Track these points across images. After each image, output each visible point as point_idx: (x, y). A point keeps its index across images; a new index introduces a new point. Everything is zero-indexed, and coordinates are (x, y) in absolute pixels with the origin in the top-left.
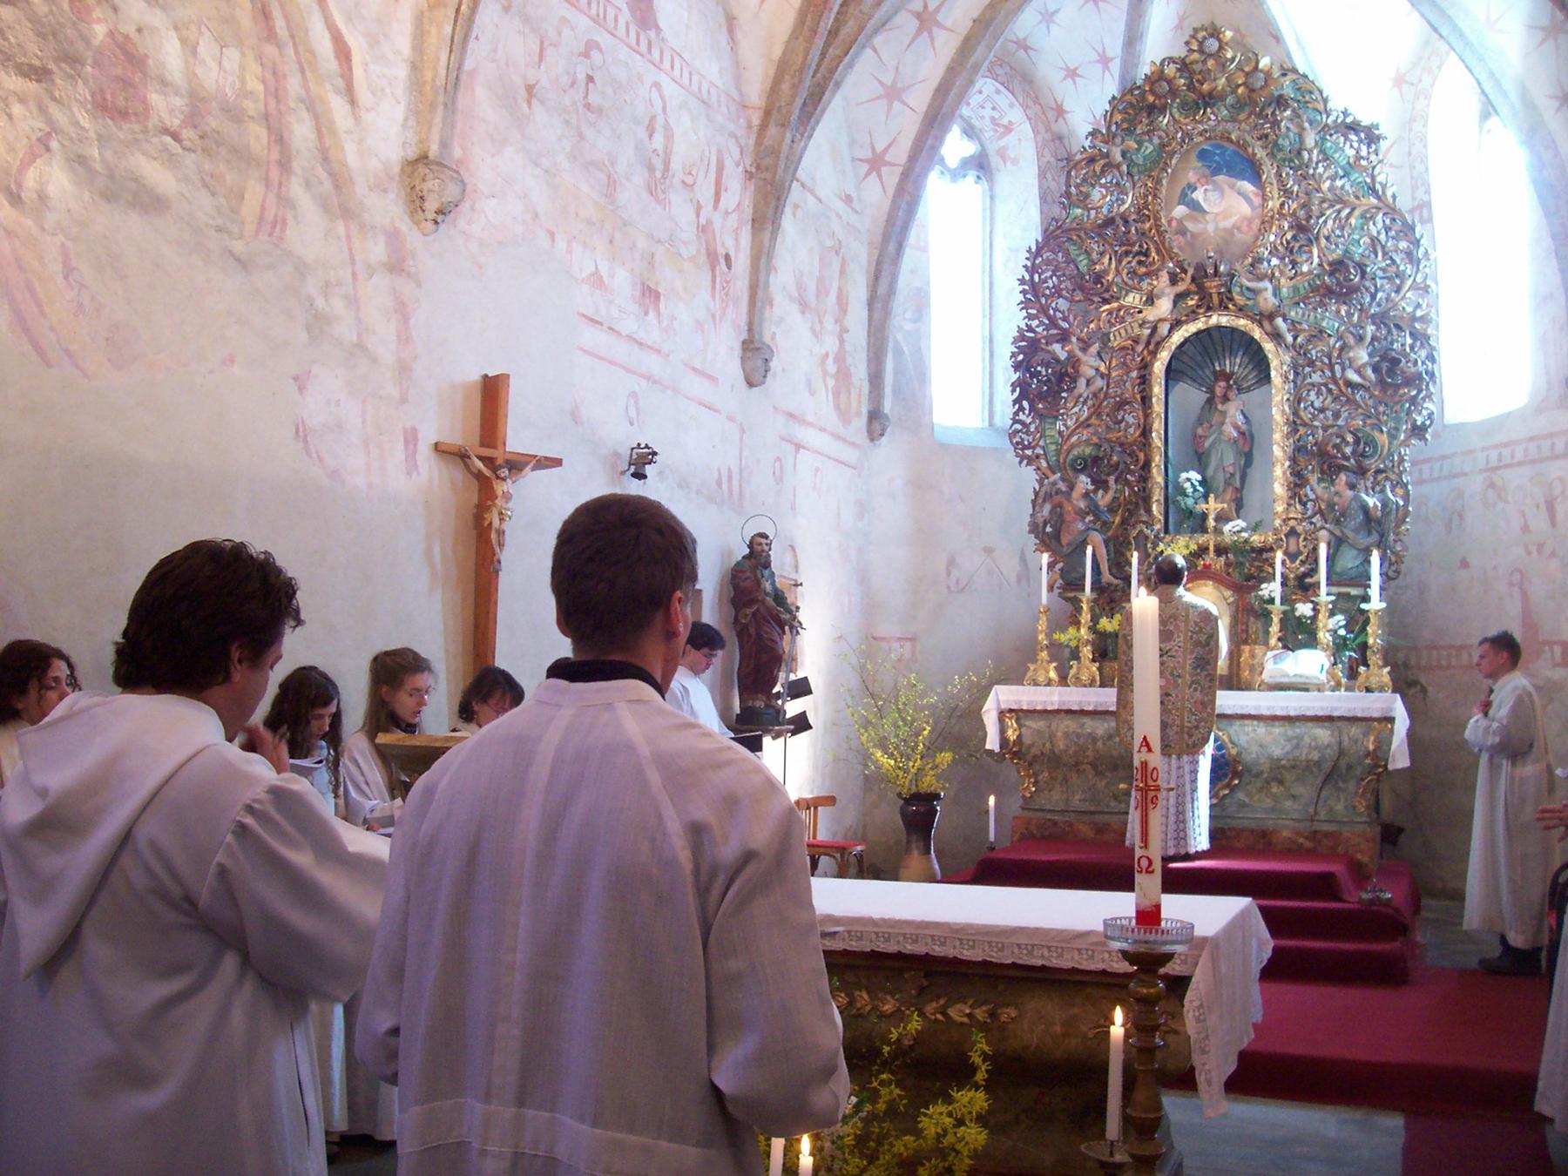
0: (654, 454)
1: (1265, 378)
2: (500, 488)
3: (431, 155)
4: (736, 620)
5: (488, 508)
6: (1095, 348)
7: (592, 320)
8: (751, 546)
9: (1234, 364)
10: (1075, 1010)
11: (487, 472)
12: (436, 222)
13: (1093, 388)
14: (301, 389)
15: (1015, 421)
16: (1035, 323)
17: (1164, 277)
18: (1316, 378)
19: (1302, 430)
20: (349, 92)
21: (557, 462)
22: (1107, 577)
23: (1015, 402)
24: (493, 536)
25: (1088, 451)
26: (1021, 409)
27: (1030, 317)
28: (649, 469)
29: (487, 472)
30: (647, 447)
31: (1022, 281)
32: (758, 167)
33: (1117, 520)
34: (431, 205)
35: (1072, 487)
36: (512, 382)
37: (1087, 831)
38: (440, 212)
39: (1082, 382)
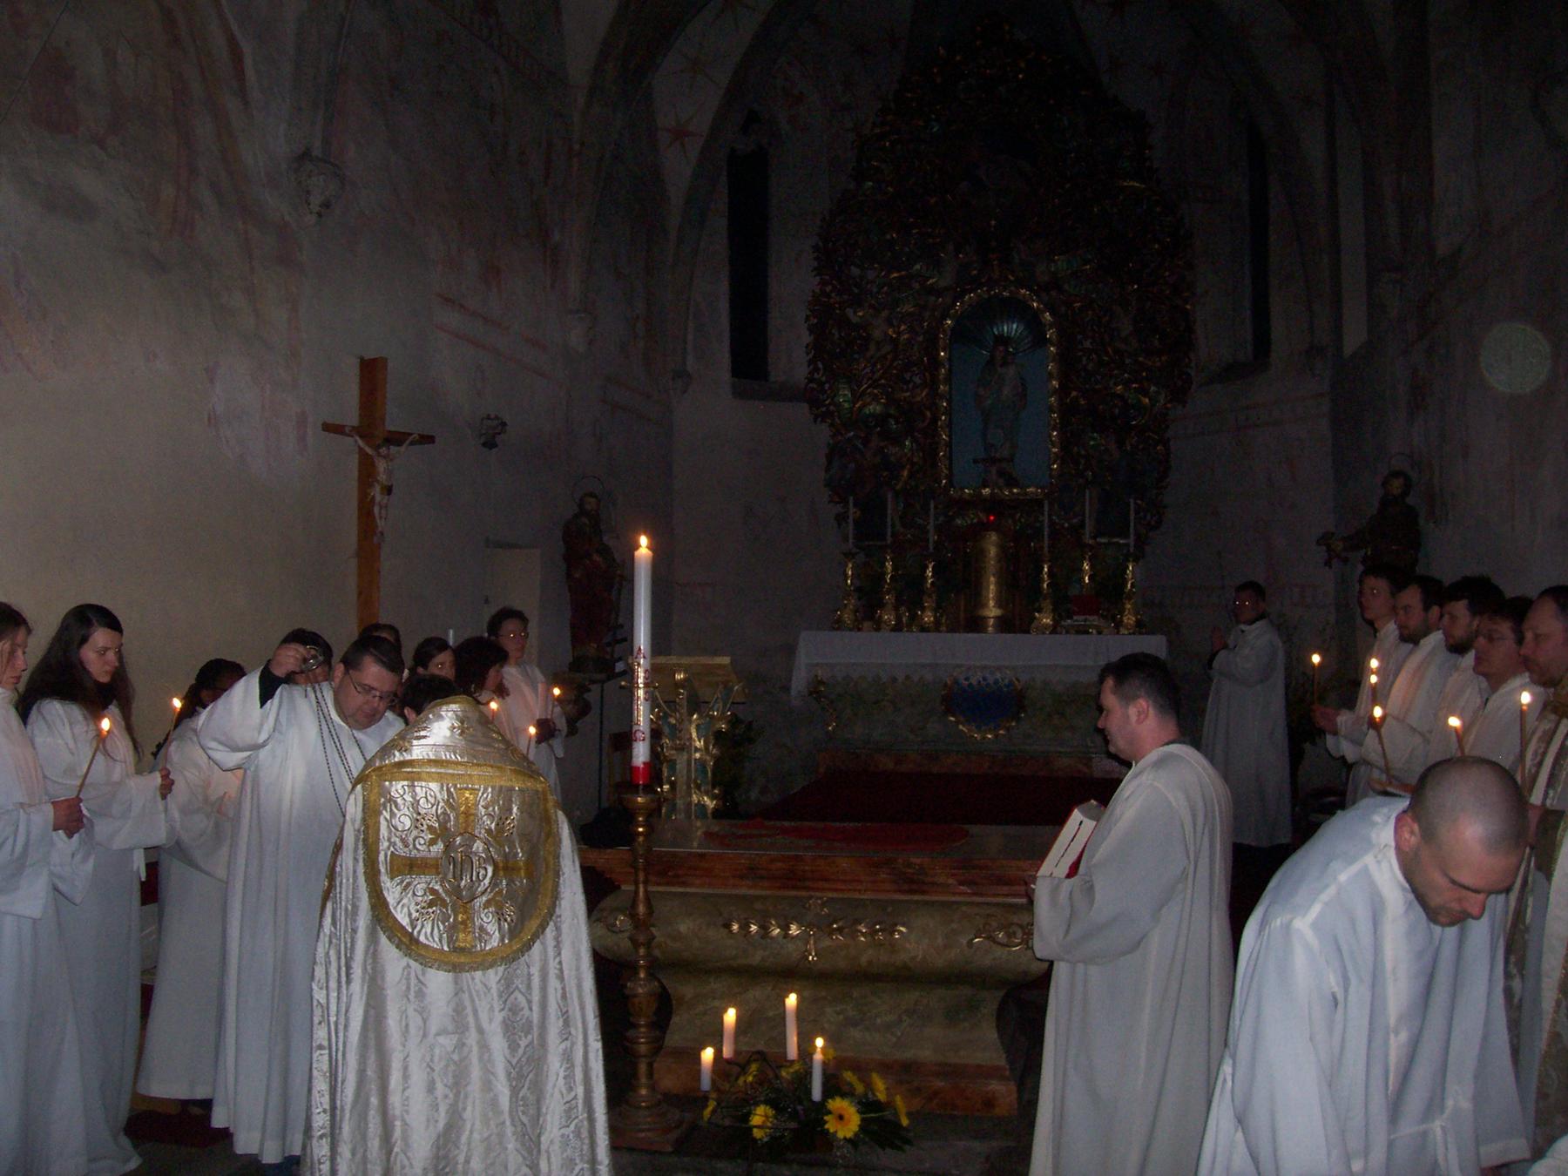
0: (504, 424)
1: (1040, 342)
2: (381, 466)
3: (317, 152)
4: (569, 575)
5: (371, 485)
6: (885, 314)
7: (448, 300)
8: (581, 505)
9: (1012, 328)
10: (954, 926)
11: (369, 450)
12: (320, 215)
13: (884, 351)
14: (212, 381)
15: (811, 380)
16: (828, 289)
17: (951, 247)
18: (1087, 344)
19: (1074, 394)
20: (242, 93)
21: (428, 439)
22: (899, 527)
23: (810, 362)
24: (376, 510)
25: (879, 408)
26: (816, 370)
27: (823, 283)
28: (498, 439)
29: (369, 450)
30: (497, 418)
31: (816, 248)
32: (582, 144)
33: (905, 473)
34: (316, 201)
35: (866, 442)
36: (390, 365)
37: (887, 763)
38: (326, 205)
39: (872, 347)
